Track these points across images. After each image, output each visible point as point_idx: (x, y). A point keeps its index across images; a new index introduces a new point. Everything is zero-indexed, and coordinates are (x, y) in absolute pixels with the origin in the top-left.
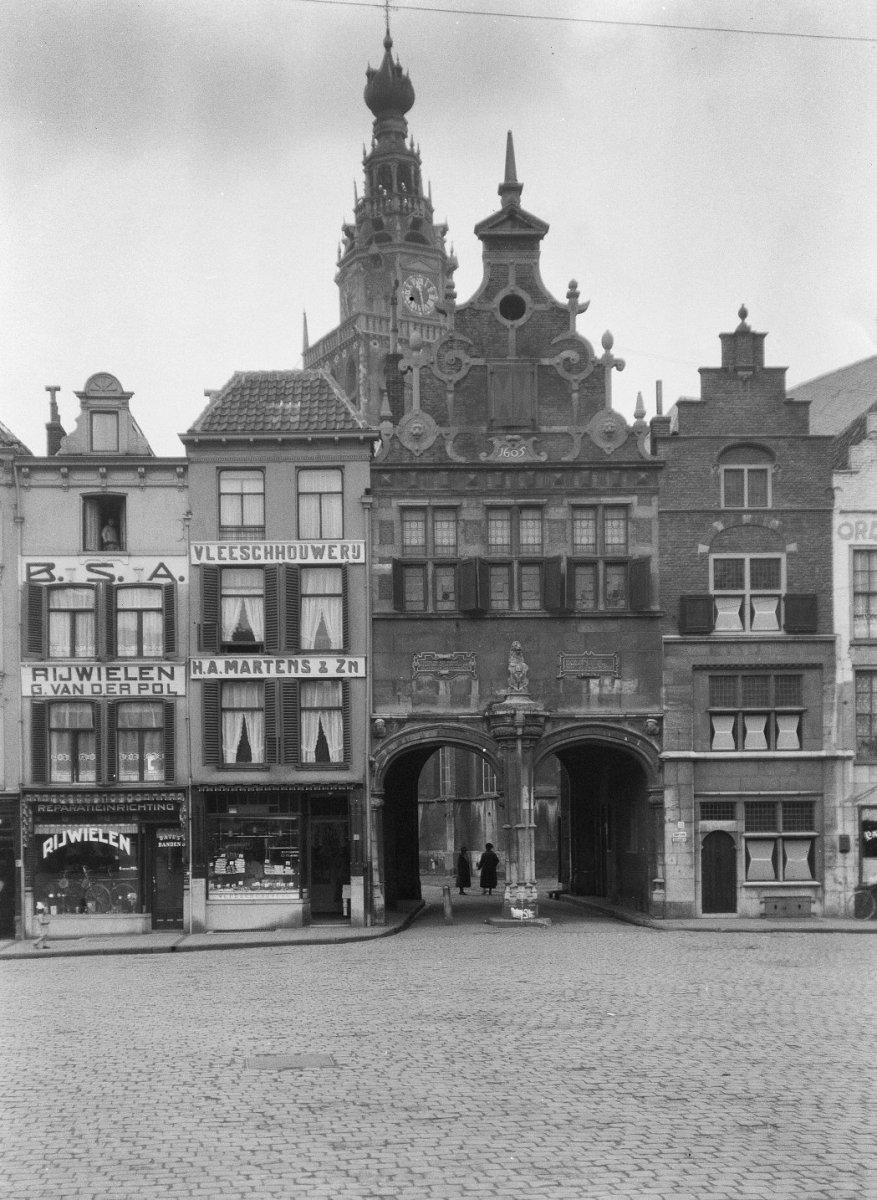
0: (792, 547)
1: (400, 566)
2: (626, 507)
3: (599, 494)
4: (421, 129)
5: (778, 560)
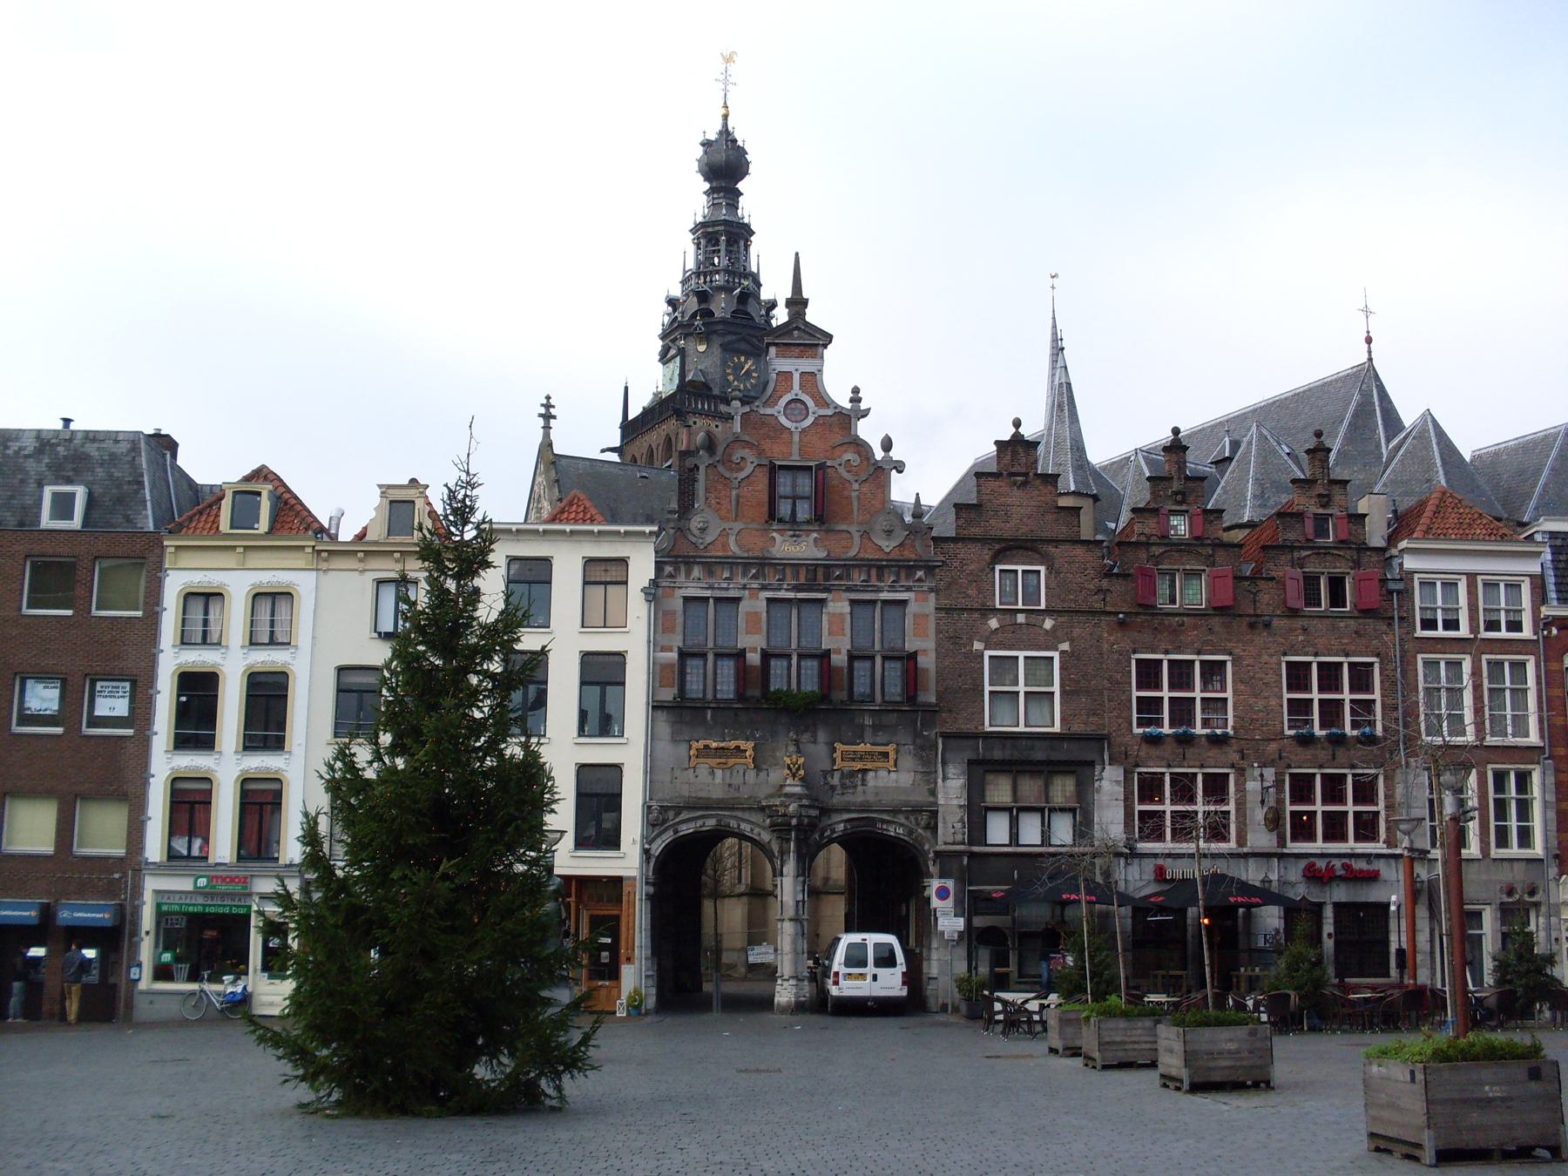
0: (1065, 646)
3: (880, 590)
4: (754, 200)
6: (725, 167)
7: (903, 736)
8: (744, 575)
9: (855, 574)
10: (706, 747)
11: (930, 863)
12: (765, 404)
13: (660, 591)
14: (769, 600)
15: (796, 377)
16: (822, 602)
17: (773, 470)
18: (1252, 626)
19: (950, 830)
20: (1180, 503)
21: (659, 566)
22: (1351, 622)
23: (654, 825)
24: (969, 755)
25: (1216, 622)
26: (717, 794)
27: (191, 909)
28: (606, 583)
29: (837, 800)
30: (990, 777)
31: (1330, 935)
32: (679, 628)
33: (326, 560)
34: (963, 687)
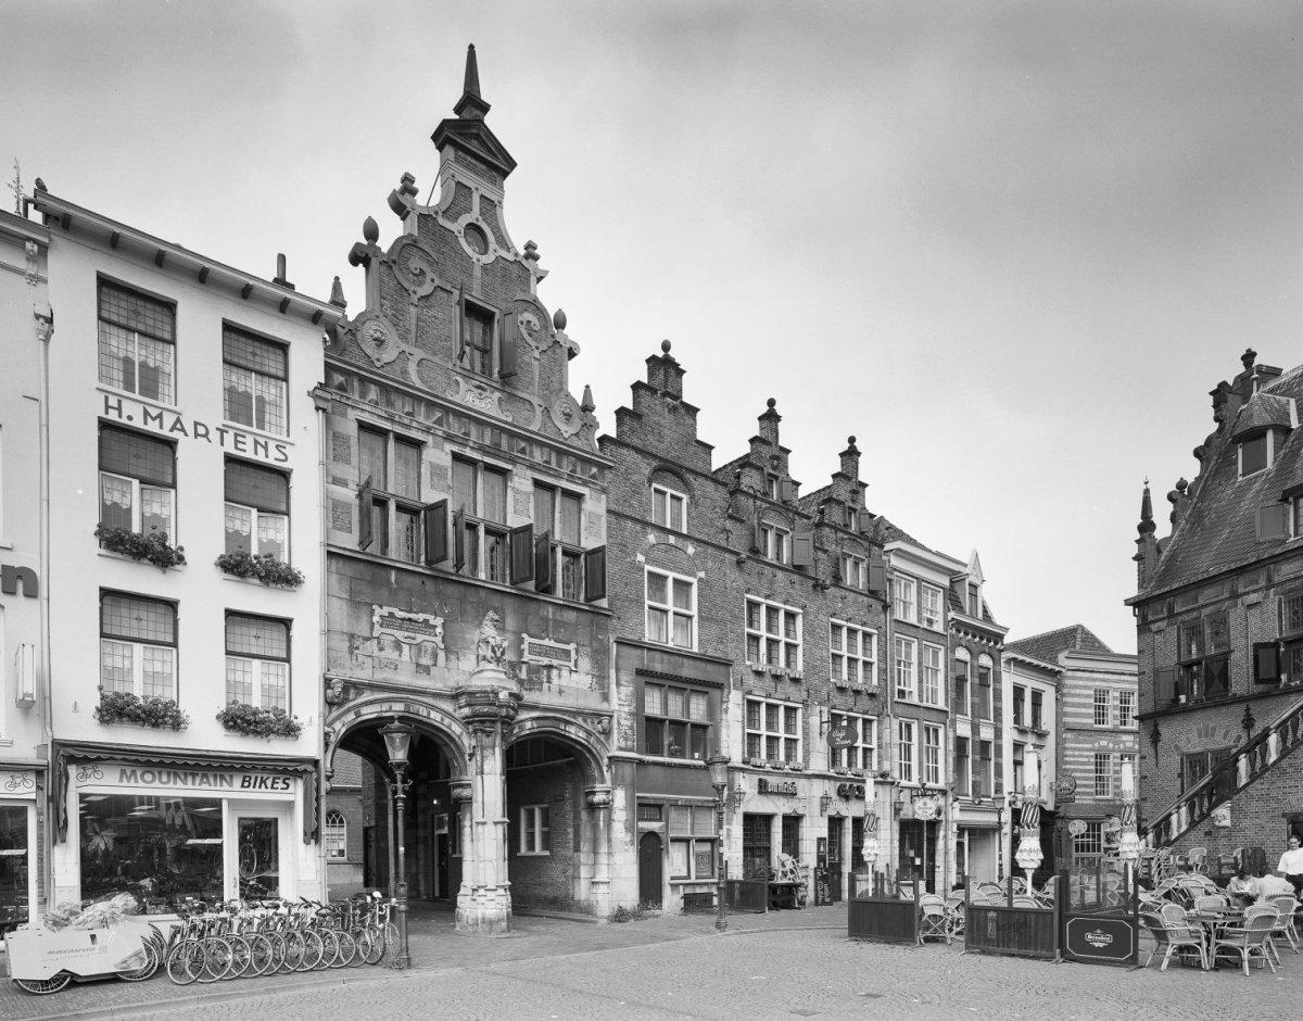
2: (579, 497)
3: (558, 476)
5: (689, 585)
7: (583, 635)
10: (391, 615)
18: (815, 586)
24: (637, 664)
25: (795, 577)
30: (648, 691)
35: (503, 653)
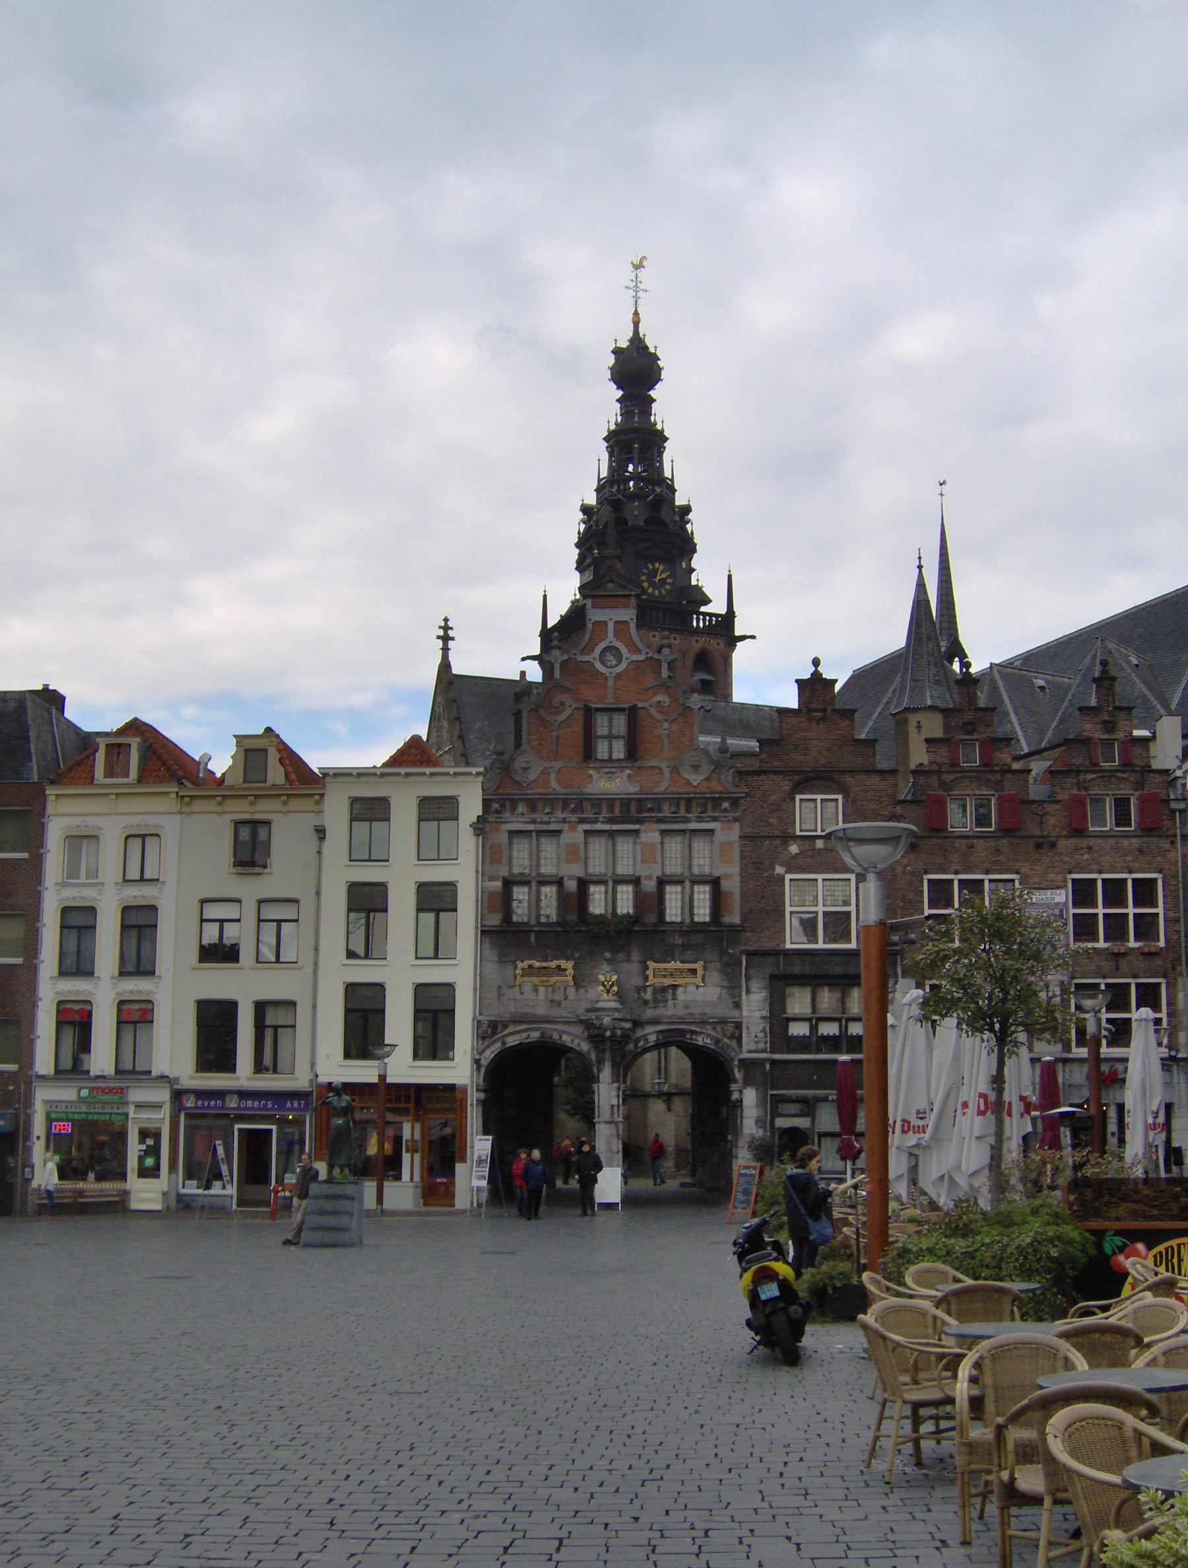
1: (508, 884)
3: (688, 821)
6: (636, 371)
8: (564, 809)
9: (666, 808)
10: (530, 966)
11: (736, 1070)
12: (583, 652)
13: (488, 826)
14: (586, 832)
15: (611, 626)
16: (636, 832)
17: (589, 714)
19: (753, 1040)
20: (971, 733)
21: (486, 804)
22: (1134, 840)
23: (484, 1038)
24: (769, 971)
26: (541, 1010)
27: (76, 1116)
28: (439, 820)
29: (649, 1013)
30: (789, 990)
31: (1113, 1134)
32: (505, 860)
33: (188, 804)
34: (766, 905)
35: (612, 986)
